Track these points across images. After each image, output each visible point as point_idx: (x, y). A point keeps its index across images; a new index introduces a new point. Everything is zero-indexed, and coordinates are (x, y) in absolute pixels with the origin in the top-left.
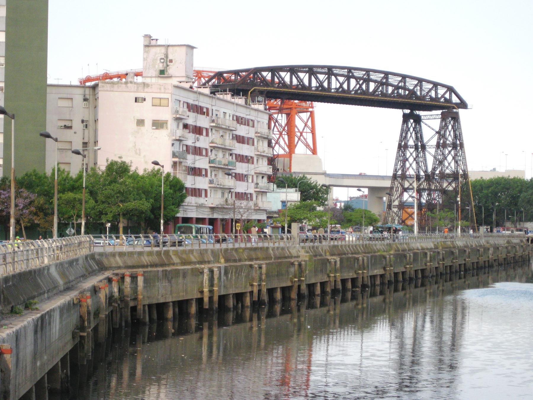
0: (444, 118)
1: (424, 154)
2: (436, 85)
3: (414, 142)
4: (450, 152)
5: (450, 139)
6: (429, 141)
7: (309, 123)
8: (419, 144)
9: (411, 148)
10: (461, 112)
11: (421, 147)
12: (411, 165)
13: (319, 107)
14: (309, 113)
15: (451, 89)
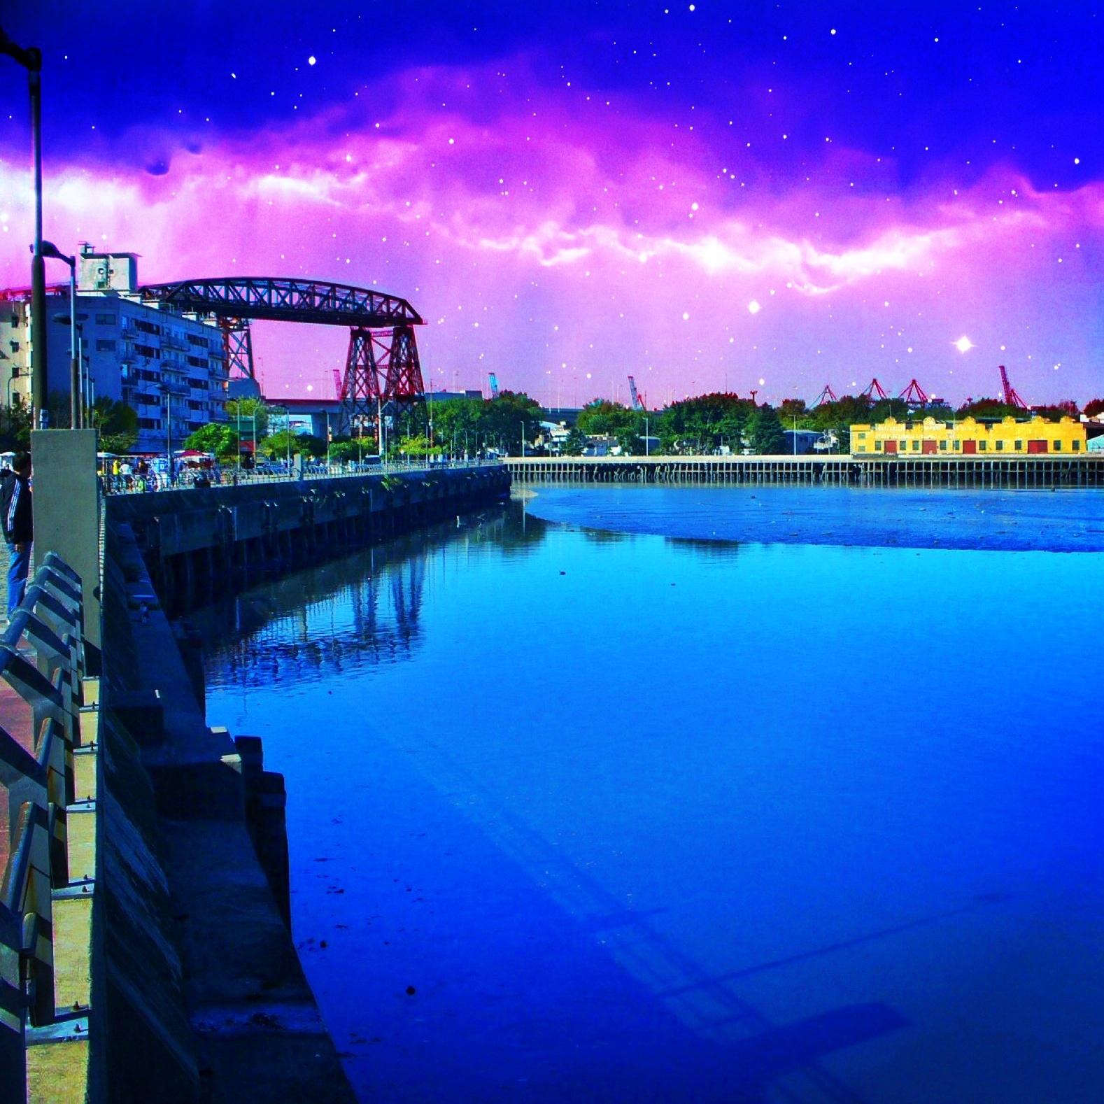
0: (397, 335)
1: (376, 377)
2: (388, 298)
3: (364, 362)
4: (404, 372)
5: (403, 358)
6: (380, 360)
7: (245, 343)
8: (370, 364)
9: (360, 368)
10: (416, 327)
11: (372, 367)
12: (361, 388)
13: (258, 326)
14: (244, 332)
15: (403, 303)
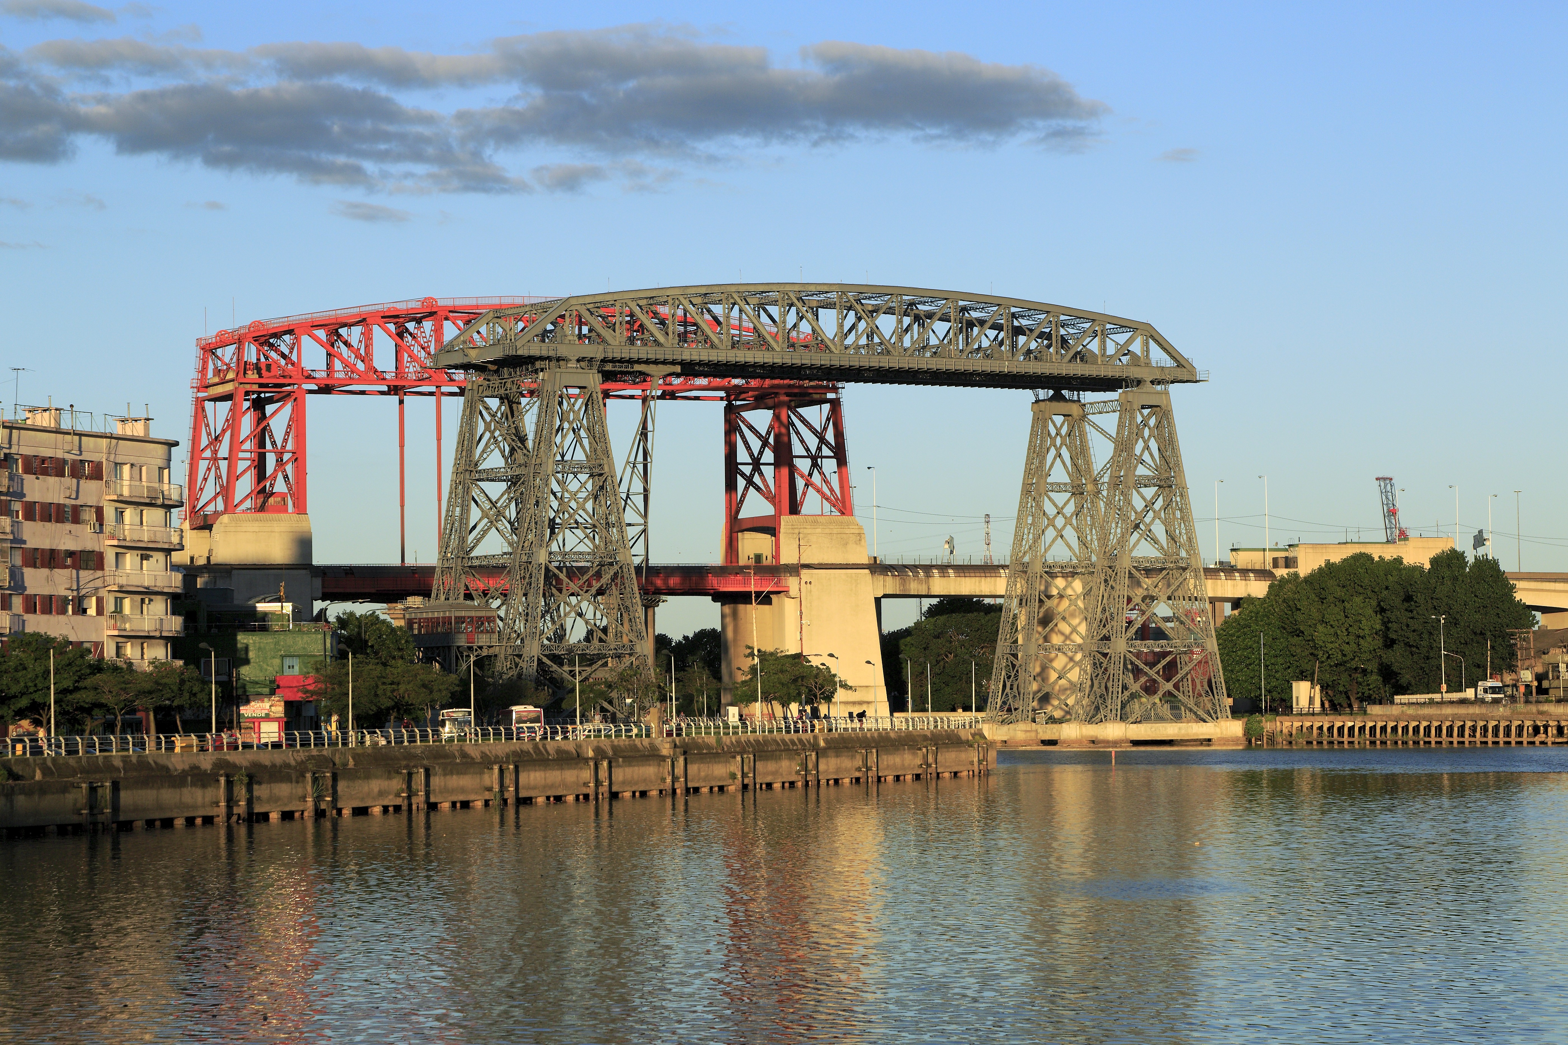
7: (830, 436)
14: (826, 407)
